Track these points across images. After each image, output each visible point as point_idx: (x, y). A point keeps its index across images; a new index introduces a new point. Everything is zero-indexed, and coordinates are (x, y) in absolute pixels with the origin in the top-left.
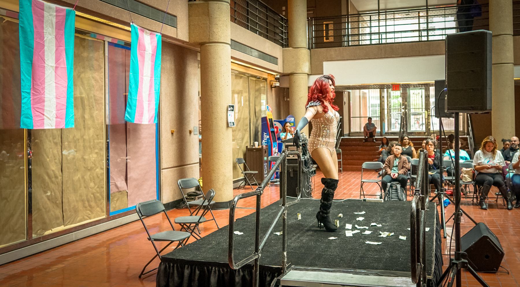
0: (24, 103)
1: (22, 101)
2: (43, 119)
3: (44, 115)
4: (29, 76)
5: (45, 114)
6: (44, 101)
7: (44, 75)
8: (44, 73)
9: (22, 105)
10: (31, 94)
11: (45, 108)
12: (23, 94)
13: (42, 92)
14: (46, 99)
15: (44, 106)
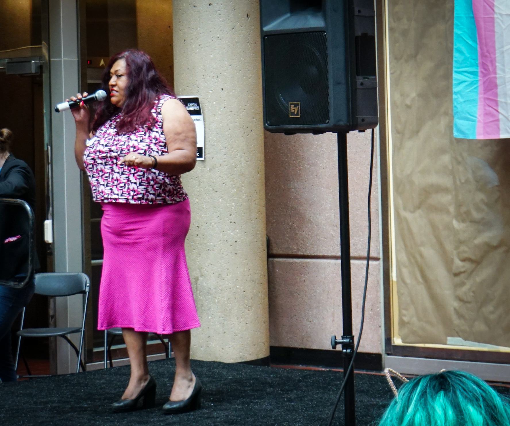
0: (456, 94)
1: (455, 89)
2: (498, 120)
3: (498, 111)
4: (474, 41)
5: (500, 110)
6: (496, 86)
7: (494, 36)
8: (493, 31)
9: (454, 97)
10: (479, 74)
11: (499, 99)
12: (455, 76)
13: (491, 69)
14: (499, 82)
15: (496, 95)
